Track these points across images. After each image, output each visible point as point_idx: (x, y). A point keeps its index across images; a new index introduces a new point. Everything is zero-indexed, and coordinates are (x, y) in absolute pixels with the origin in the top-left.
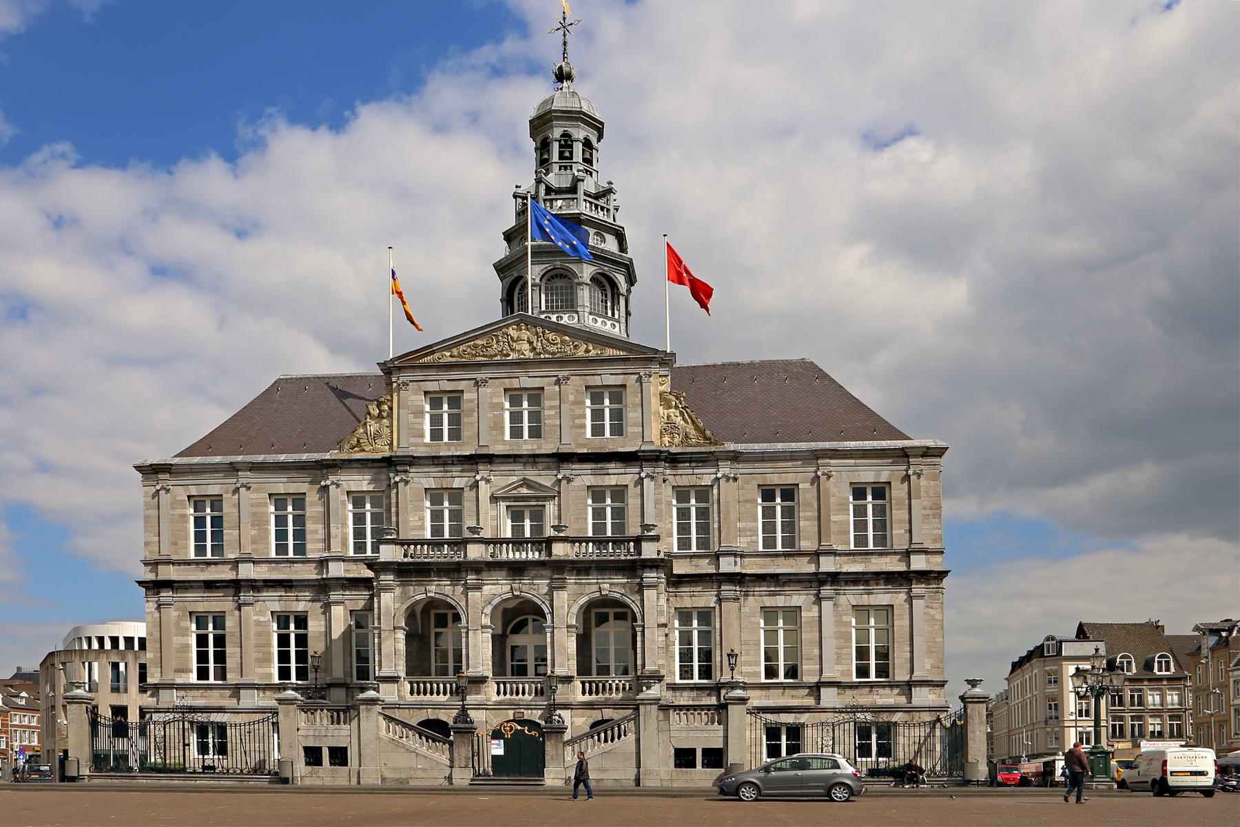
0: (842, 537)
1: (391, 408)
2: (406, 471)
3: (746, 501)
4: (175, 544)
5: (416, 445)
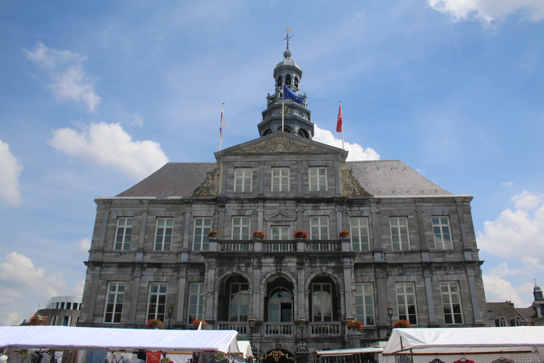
1: (219, 175)
3: (385, 225)
5: (229, 193)
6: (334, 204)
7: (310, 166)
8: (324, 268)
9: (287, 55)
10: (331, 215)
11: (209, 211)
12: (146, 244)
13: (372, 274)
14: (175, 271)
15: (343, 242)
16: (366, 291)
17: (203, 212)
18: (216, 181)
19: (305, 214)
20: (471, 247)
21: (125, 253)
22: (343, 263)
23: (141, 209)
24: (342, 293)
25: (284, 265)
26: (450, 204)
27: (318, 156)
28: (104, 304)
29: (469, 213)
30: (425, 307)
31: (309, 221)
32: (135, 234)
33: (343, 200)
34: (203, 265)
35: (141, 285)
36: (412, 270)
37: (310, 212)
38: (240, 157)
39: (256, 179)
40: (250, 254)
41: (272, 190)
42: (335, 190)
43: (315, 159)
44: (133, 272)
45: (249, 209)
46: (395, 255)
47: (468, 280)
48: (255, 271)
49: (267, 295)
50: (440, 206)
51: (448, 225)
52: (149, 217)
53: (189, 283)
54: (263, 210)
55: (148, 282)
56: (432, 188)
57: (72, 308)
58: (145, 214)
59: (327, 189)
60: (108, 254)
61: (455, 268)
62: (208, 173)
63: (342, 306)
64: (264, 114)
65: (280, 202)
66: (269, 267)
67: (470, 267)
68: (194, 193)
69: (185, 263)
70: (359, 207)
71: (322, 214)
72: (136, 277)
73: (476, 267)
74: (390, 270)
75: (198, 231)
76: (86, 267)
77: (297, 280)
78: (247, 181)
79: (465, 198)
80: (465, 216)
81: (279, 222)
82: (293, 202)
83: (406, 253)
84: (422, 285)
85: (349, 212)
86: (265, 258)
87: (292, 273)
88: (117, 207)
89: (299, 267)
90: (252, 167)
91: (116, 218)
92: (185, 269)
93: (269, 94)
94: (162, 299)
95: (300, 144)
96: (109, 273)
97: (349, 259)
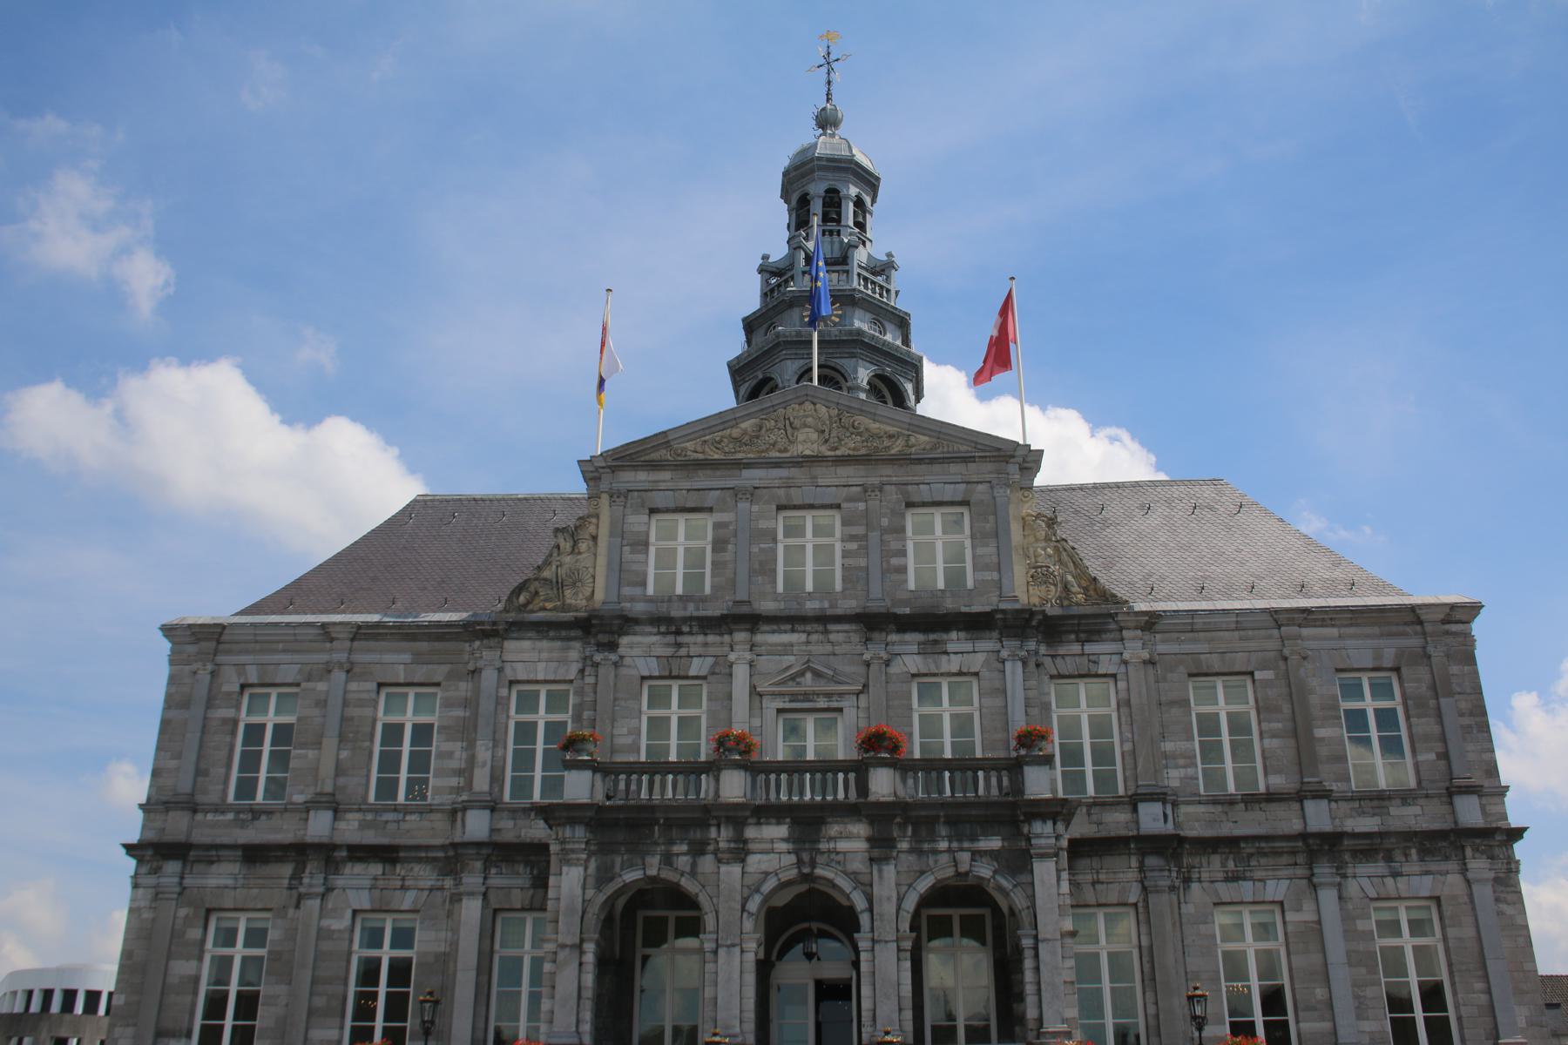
1: (595, 538)
3: (1172, 703)
5: (632, 599)
6: (995, 634)
7: (910, 505)
8: (965, 857)
9: (826, 121)
10: (985, 673)
11: (563, 661)
12: (342, 781)
13: (1132, 875)
14: (444, 873)
15: (1028, 764)
16: (1112, 936)
17: (541, 666)
18: (585, 559)
19: (895, 669)
20: (1477, 779)
21: (269, 813)
22: (1029, 839)
23: (324, 657)
24: (1027, 942)
25: (823, 846)
26: (1401, 628)
27: (937, 468)
28: (195, 993)
29: (1470, 659)
30: (1320, 993)
31: (910, 693)
32: (303, 746)
33: (1028, 621)
34: (542, 848)
35: (325, 923)
36: (1271, 861)
37: (913, 663)
38: (666, 475)
39: (724, 550)
40: (706, 809)
41: (780, 588)
42: (999, 585)
43: (928, 479)
44: (297, 876)
45: (700, 654)
46: (1211, 808)
47: (1471, 896)
48: (723, 868)
49: (768, 952)
50: (1368, 636)
51: (1396, 703)
52: (353, 686)
53: (492, 914)
54: (748, 656)
55: (349, 914)
56: (1338, 574)
57: (79, 1008)
58: (339, 676)
59: (970, 584)
60: (210, 817)
61: (1424, 853)
62: (557, 530)
63: (1029, 989)
64: (750, 325)
65: (808, 628)
67: (1476, 849)
68: (509, 599)
69: (478, 845)
70: (1083, 642)
71: (955, 669)
72: (309, 896)
73: (1497, 851)
74: (1196, 861)
75: (526, 732)
76: (132, 863)
77: (870, 899)
78: (695, 559)
79: (1453, 607)
80: (1454, 669)
81: (807, 696)
82: (853, 627)
83: (1251, 800)
84: (1307, 915)
85: (1048, 661)
86: (759, 824)
87: (854, 876)
88: (240, 652)
89: (876, 853)
90: (710, 510)
91: (237, 689)
92: (479, 865)
93: (765, 257)
94: (400, 971)
95: (874, 426)
96: (212, 882)
97: (1050, 824)
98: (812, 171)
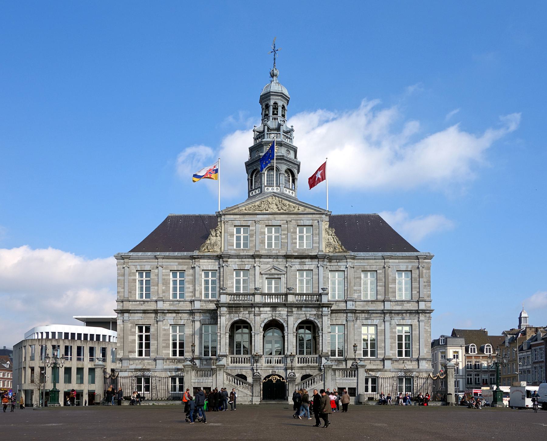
0: (394, 294)
2: (227, 261)
3: (357, 278)
4: (130, 292)
5: (231, 250)
12: (164, 294)
21: (148, 302)
24: (320, 334)
32: (154, 286)
45: (248, 264)
52: (164, 271)
66: (266, 315)
69: (198, 310)
98: (270, 96)
